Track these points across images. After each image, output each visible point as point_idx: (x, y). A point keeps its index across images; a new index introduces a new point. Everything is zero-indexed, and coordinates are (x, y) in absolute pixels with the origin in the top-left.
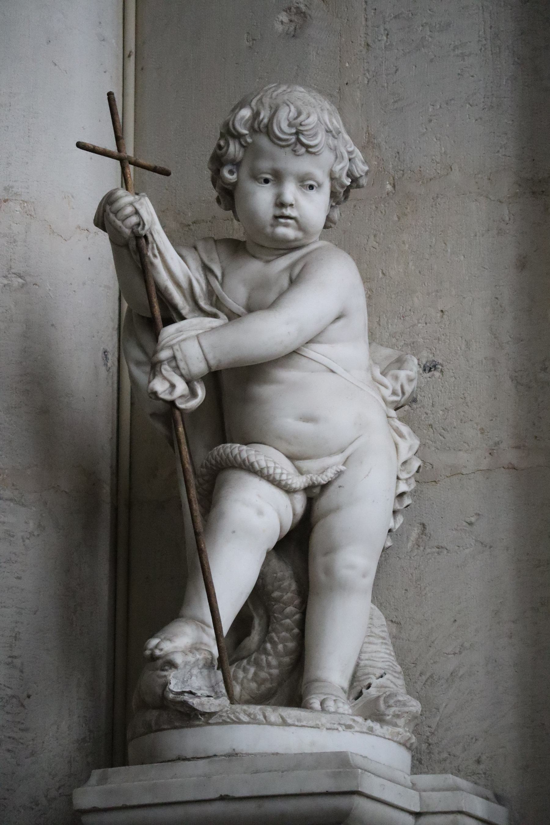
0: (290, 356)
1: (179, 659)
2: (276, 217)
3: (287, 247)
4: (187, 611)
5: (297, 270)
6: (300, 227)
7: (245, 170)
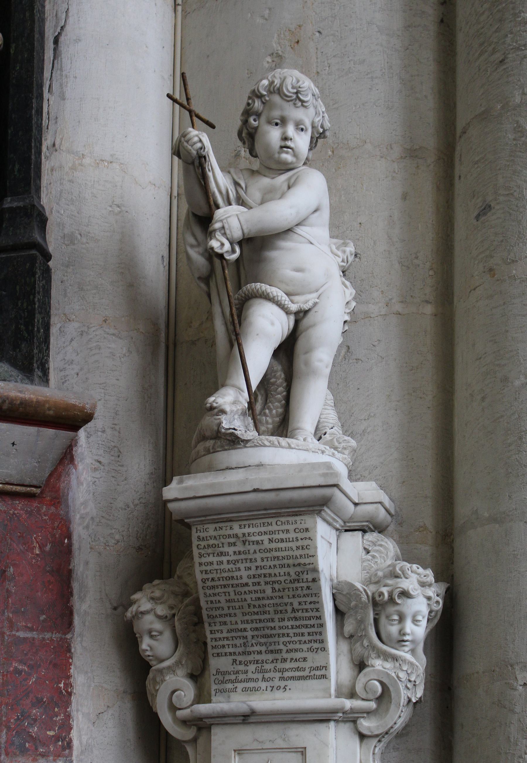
0: (287, 232)
3: (286, 168)
5: (292, 181)
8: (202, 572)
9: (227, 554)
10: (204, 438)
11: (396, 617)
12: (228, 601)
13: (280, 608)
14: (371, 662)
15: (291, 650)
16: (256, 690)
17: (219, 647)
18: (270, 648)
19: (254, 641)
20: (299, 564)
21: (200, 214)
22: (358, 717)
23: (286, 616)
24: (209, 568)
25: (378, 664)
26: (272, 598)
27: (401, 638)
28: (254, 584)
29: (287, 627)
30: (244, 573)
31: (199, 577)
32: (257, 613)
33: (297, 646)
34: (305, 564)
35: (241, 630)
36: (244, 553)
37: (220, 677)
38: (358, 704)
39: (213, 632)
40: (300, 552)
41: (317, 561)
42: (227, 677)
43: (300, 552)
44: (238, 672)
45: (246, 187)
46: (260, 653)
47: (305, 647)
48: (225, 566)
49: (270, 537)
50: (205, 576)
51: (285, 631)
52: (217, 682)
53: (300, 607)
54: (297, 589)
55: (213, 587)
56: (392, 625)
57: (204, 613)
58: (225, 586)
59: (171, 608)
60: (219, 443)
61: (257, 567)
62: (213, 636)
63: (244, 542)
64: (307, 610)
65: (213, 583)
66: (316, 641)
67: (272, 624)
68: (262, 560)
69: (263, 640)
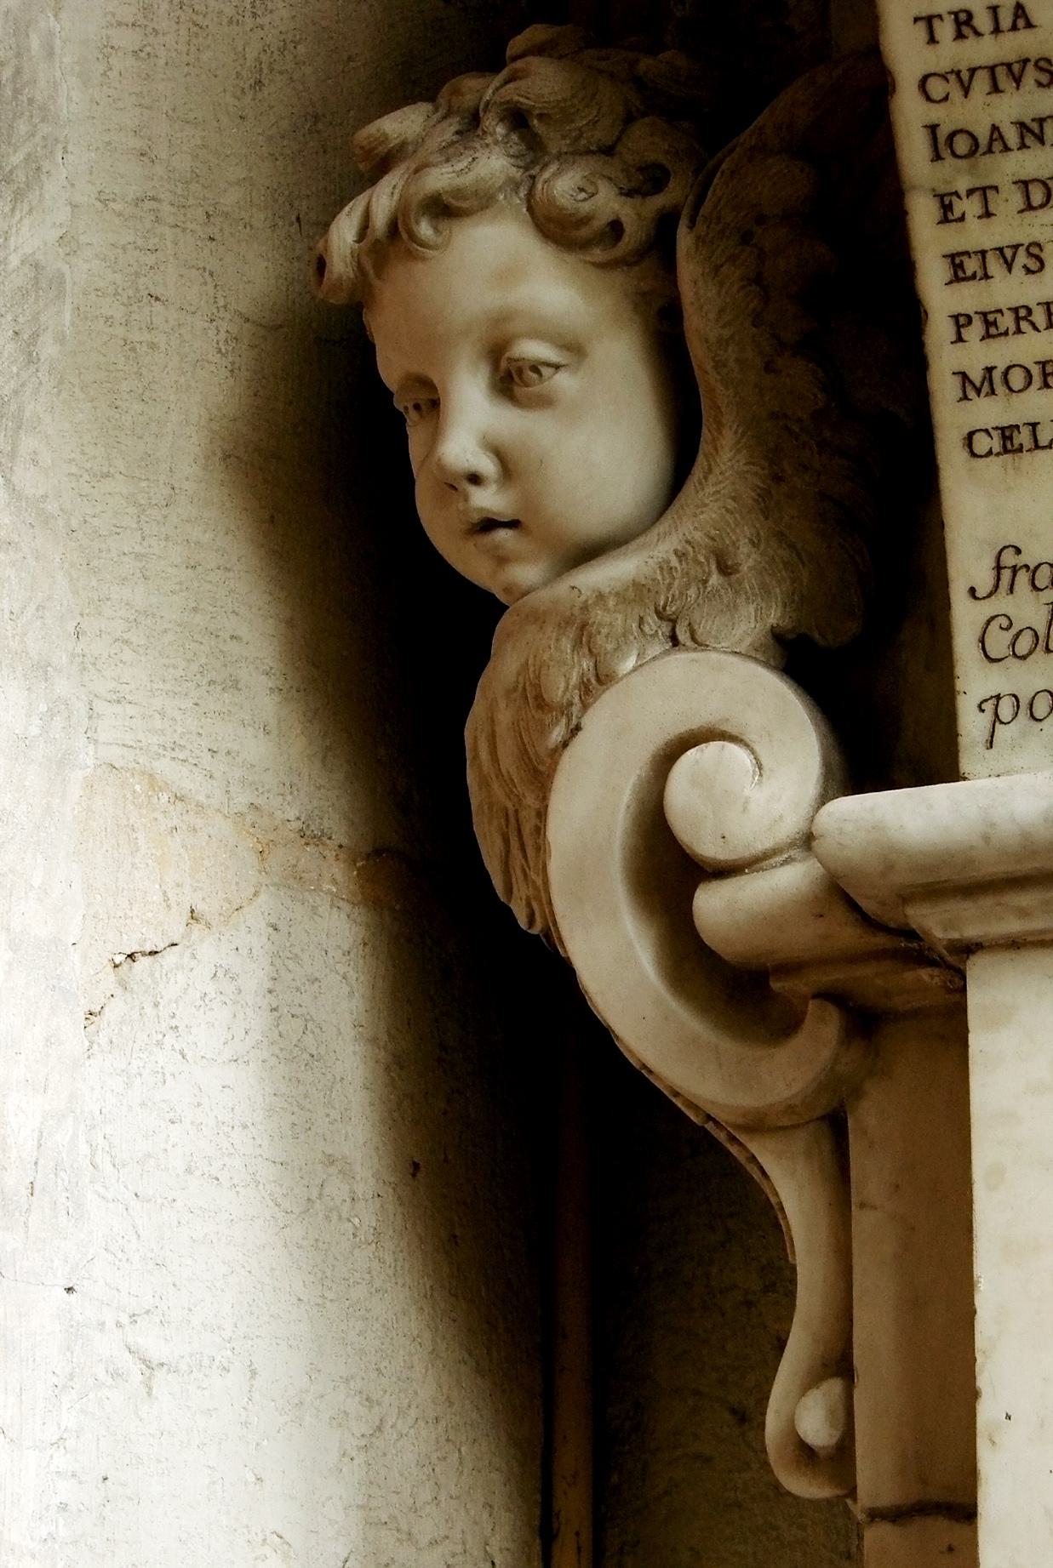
17: (1017, 379)
39: (971, 265)
52: (998, 642)
57: (911, 116)
59: (648, 180)
62: (969, 298)
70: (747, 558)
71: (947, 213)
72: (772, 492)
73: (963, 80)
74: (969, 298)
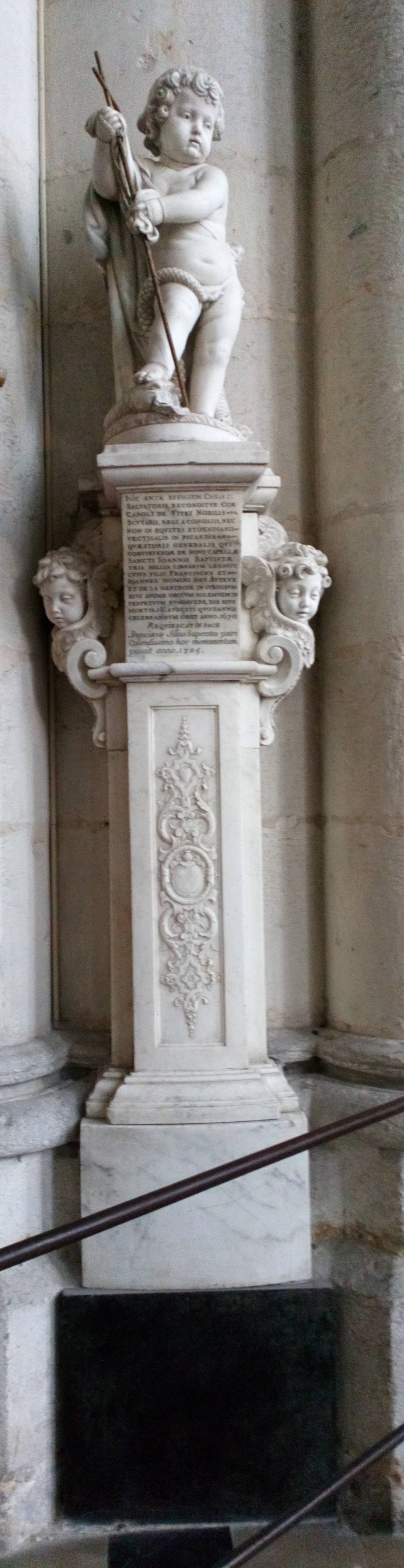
1: (161, 383)
2: (191, 141)
3: (190, 161)
4: (155, 360)
5: (200, 174)
6: (201, 151)
7: (174, 110)
8: (129, 538)
9: (155, 523)
10: (133, 411)
11: (297, 591)
12: (151, 568)
13: (199, 577)
14: (272, 630)
15: (206, 617)
16: (170, 651)
18: (187, 614)
19: (171, 607)
20: (224, 537)
21: (104, 195)
22: (260, 680)
23: (204, 584)
24: (137, 535)
25: (280, 632)
26: (194, 566)
27: (301, 610)
28: (179, 553)
29: (204, 595)
30: (171, 542)
31: (126, 542)
32: (178, 581)
33: (211, 613)
34: (229, 537)
35: (159, 596)
36: (173, 523)
37: (135, 639)
38: (262, 668)
40: (226, 525)
41: (240, 534)
42: (143, 639)
43: (226, 525)
44: (153, 635)
45: (152, 175)
46: (176, 617)
47: (218, 614)
48: (153, 534)
49: (199, 509)
50: (132, 543)
51: (202, 598)
53: (220, 576)
54: (219, 559)
55: (139, 554)
56: (292, 598)
58: (150, 553)
60: (152, 415)
61: (184, 537)
62: (131, 600)
63: (173, 513)
64: (224, 580)
65: (139, 550)
66: (229, 609)
67: (190, 592)
68: (190, 530)
69: (180, 606)
70: (94, 625)
71: (130, 589)
72: (98, 617)
73: (134, 574)
74: (131, 600)
